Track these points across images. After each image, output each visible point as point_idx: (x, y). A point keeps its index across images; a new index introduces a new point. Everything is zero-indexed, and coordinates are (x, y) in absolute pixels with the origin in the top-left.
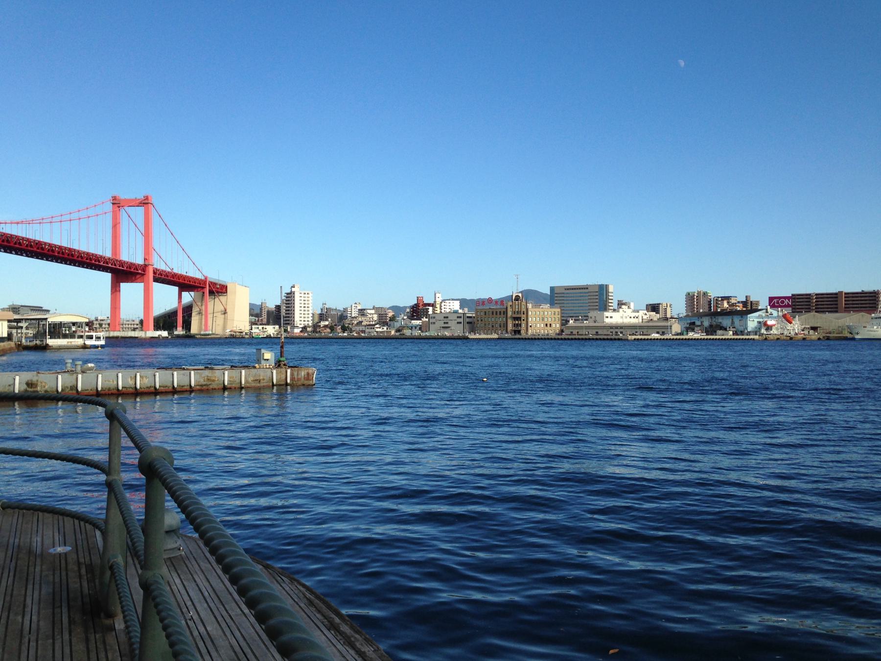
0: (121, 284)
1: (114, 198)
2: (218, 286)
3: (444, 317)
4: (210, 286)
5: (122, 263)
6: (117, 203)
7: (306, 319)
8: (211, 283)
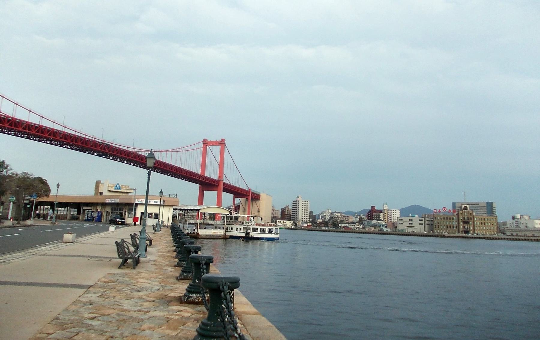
1: (205, 140)
2: (256, 195)
3: (410, 220)
4: (251, 195)
5: (207, 178)
6: (206, 143)
7: (306, 218)
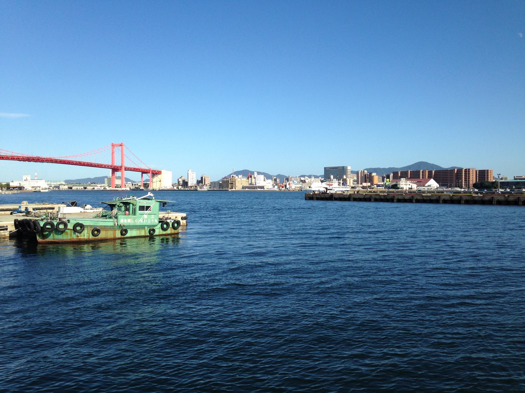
1: (112, 144)
6: (113, 146)
8: (153, 171)
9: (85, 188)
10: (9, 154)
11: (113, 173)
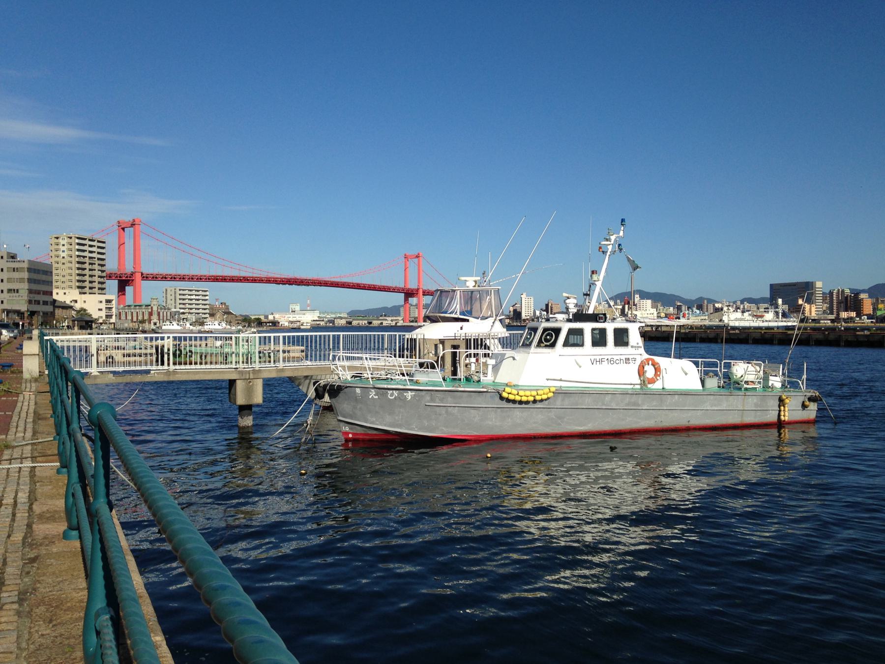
0: (410, 299)
1: (405, 255)
6: (406, 257)
9: (370, 323)
10: (264, 275)
11: (406, 300)
